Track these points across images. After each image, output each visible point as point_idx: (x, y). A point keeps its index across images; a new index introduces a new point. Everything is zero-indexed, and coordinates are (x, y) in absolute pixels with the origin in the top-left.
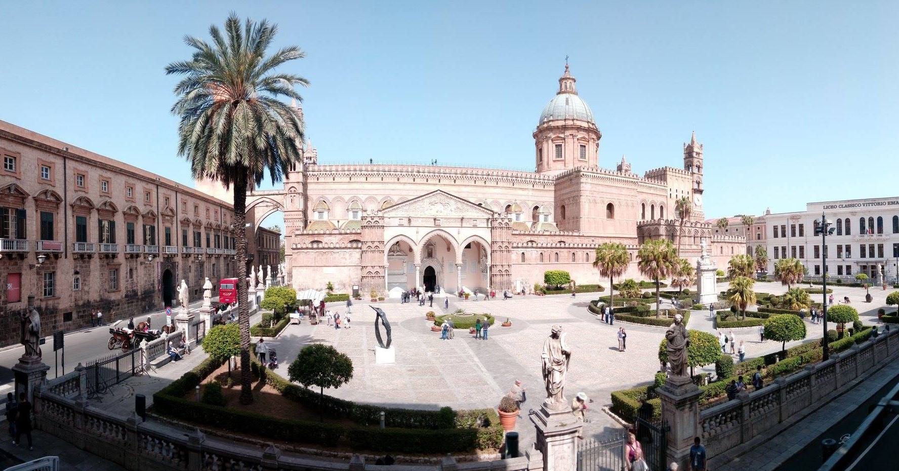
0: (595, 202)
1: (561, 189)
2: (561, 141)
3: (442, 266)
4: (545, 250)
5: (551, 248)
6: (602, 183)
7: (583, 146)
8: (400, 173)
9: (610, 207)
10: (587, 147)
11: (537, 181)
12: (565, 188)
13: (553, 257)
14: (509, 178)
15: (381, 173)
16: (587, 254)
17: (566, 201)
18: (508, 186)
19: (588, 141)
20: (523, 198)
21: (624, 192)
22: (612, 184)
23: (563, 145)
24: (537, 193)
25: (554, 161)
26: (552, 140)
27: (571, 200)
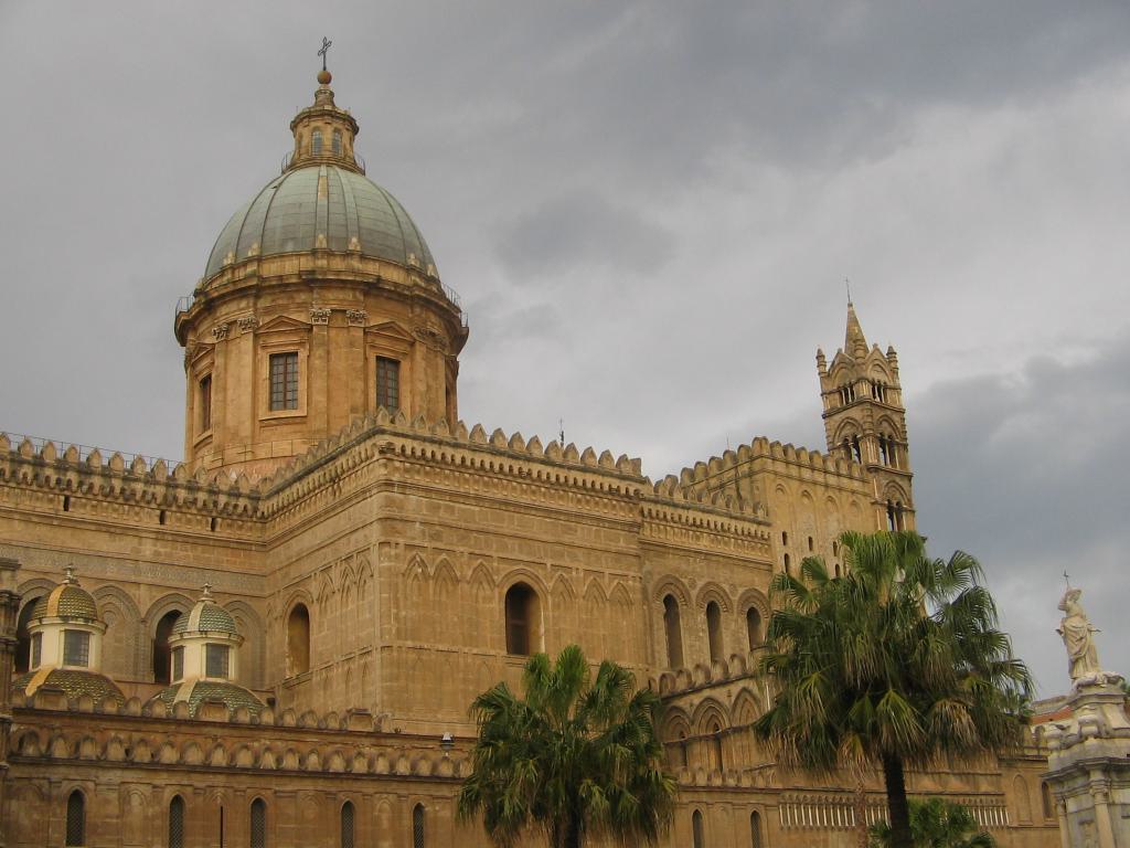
0: (446, 575)
1: (291, 534)
2: (295, 339)
4: (199, 781)
5: (231, 770)
6: (481, 490)
7: (388, 364)
9: (520, 599)
10: (405, 365)
12: (308, 524)
13: (239, 823)
14: (49, 472)
16: (419, 809)
17: (314, 588)
18: (43, 507)
19: (412, 344)
20: (112, 571)
21: (583, 535)
22: (526, 499)
23: (303, 354)
24: (184, 554)
25: (265, 424)
27: (335, 573)
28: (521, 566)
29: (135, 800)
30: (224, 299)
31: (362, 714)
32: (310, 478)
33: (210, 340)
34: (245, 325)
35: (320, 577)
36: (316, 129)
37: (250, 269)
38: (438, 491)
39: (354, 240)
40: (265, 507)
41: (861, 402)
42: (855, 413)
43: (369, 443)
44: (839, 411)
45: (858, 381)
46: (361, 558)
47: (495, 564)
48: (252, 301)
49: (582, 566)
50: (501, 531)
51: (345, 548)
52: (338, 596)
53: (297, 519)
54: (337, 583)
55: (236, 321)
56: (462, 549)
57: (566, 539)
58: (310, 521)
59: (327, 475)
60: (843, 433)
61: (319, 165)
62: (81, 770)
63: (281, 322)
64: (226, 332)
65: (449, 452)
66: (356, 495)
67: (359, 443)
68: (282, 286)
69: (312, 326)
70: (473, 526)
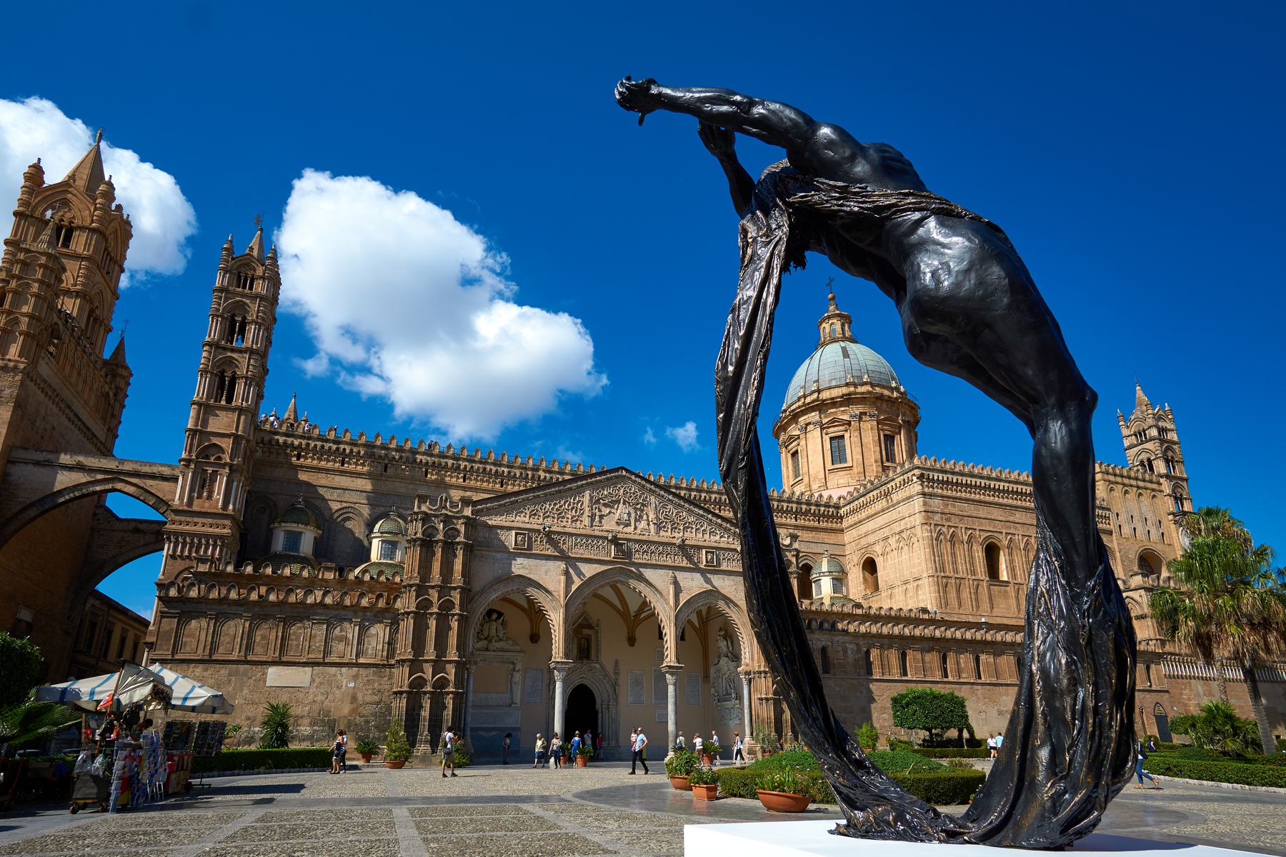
3: (615, 685)
8: (506, 470)
9: (992, 552)
11: (804, 507)
15: (463, 464)
17: (878, 548)
23: (847, 435)
26: (822, 429)
27: (892, 541)
28: (988, 534)
29: (849, 652)
30: (803, 413)
31: (925, 611)
32: (871, 494)
33: (798, 433)
34: (815, 424)
35: (881, 543)
36: (832, 324)
37: (815, 395)
38: (948, 497)
39: (866, 376)
40: (841, 512)
41: (1152, 439)
42: (1149, 445)
43: (910, 474)
44: (1136, 446)
45: (1150, 427)
46: (909, 532)
47: (978, 533)
48: (818, 413)
49: (1021, 533)
50: (979, 516)
51: (897, 528)
52: (895, 552)
53: (863, 515)
54: (894, 545)
55: (809, 424)
56: (961, 525)
57: (1011, 519)
58: (872, 516)
59: (883, 493)
60: (1140, 457)
61: (838, 341)
62: (825, 636)
63: (833, 421)
64: (805, 429)
65: (950, 476)
66: (903, 501)
67: (903, 474)
68: (833, 403)
69: (850, 421)
70: (965, 514)
